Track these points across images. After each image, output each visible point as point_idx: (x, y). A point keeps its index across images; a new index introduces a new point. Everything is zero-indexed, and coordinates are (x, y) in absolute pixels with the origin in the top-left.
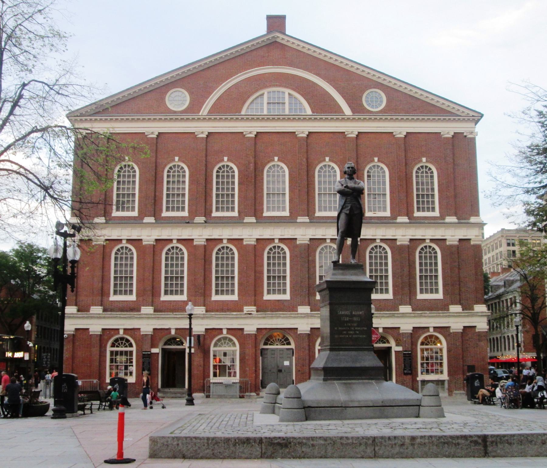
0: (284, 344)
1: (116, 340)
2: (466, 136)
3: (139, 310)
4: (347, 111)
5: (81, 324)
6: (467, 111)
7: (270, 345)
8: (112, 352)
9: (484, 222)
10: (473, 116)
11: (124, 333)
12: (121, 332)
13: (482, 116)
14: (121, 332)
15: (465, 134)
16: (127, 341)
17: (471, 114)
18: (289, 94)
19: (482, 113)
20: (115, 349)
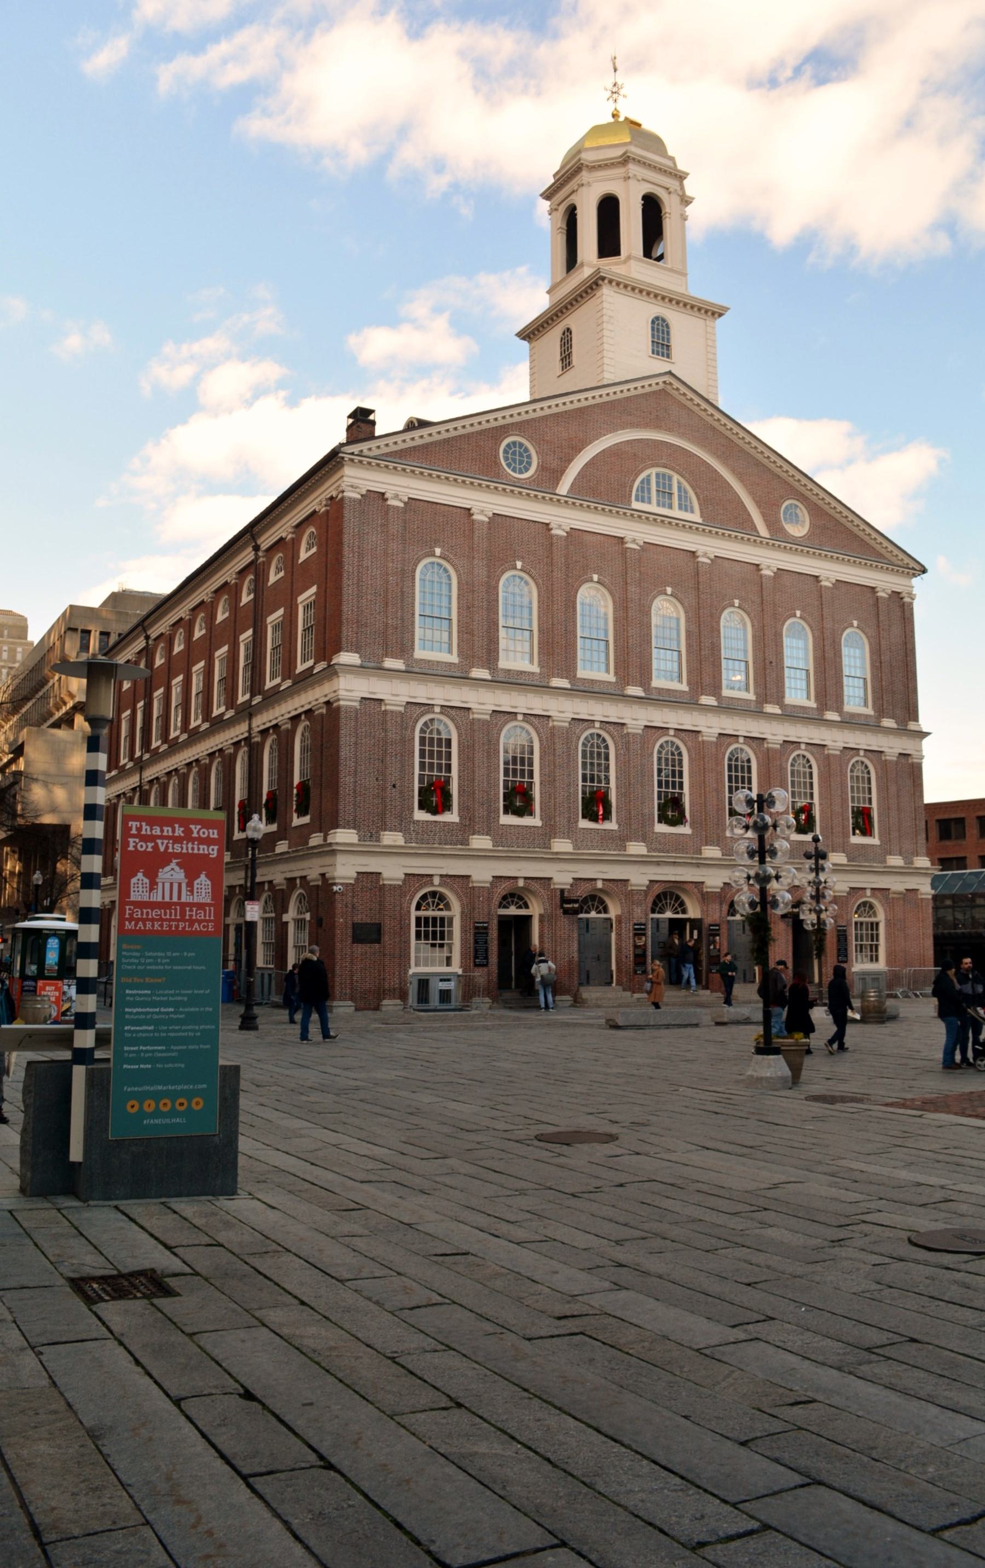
0: (678, 913)
1: (424, 897)
2: (902, 598)
3: (465, 842)
4: (763, 531)
5: (372, 864)
6: (907, 560)
7: (659, 913)
8: (418, 920)
9: (925, 730)
10: (913, 569)
11: (440, 885)
12: (436, 881)
13: (924, 571)
14: (436, 881)
15: (902, 596)
16: (442, 898)
17: (912, 564)
18: (679, 483)
19: (927, 567)
20: (422, 913)
